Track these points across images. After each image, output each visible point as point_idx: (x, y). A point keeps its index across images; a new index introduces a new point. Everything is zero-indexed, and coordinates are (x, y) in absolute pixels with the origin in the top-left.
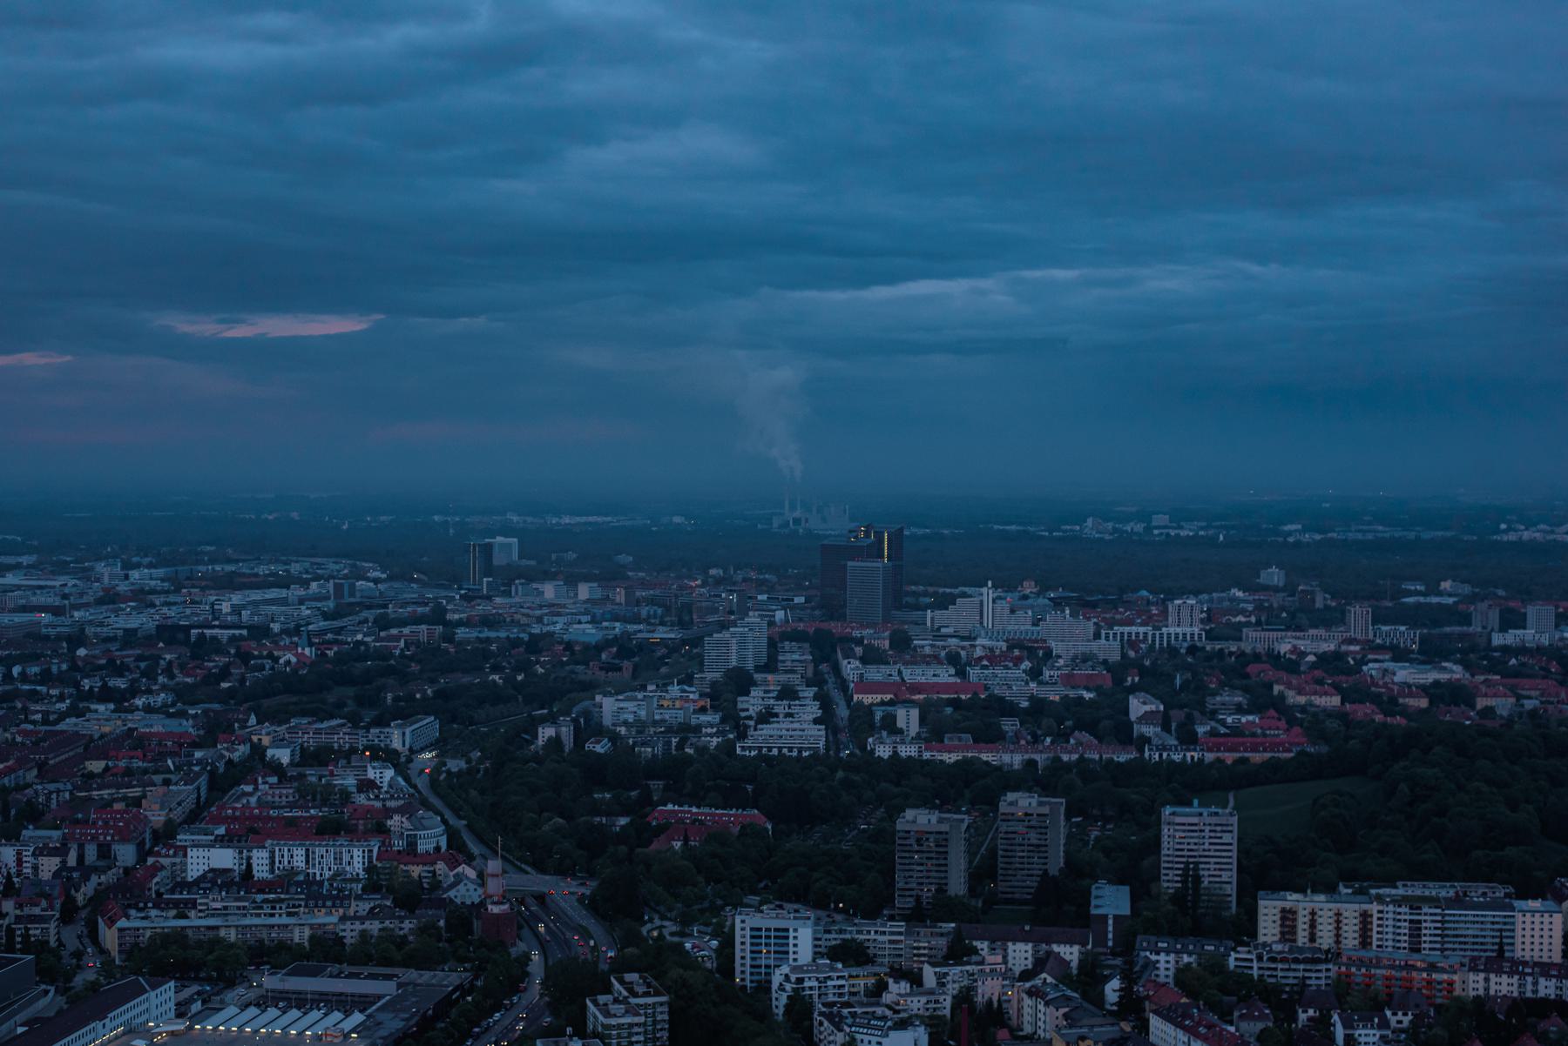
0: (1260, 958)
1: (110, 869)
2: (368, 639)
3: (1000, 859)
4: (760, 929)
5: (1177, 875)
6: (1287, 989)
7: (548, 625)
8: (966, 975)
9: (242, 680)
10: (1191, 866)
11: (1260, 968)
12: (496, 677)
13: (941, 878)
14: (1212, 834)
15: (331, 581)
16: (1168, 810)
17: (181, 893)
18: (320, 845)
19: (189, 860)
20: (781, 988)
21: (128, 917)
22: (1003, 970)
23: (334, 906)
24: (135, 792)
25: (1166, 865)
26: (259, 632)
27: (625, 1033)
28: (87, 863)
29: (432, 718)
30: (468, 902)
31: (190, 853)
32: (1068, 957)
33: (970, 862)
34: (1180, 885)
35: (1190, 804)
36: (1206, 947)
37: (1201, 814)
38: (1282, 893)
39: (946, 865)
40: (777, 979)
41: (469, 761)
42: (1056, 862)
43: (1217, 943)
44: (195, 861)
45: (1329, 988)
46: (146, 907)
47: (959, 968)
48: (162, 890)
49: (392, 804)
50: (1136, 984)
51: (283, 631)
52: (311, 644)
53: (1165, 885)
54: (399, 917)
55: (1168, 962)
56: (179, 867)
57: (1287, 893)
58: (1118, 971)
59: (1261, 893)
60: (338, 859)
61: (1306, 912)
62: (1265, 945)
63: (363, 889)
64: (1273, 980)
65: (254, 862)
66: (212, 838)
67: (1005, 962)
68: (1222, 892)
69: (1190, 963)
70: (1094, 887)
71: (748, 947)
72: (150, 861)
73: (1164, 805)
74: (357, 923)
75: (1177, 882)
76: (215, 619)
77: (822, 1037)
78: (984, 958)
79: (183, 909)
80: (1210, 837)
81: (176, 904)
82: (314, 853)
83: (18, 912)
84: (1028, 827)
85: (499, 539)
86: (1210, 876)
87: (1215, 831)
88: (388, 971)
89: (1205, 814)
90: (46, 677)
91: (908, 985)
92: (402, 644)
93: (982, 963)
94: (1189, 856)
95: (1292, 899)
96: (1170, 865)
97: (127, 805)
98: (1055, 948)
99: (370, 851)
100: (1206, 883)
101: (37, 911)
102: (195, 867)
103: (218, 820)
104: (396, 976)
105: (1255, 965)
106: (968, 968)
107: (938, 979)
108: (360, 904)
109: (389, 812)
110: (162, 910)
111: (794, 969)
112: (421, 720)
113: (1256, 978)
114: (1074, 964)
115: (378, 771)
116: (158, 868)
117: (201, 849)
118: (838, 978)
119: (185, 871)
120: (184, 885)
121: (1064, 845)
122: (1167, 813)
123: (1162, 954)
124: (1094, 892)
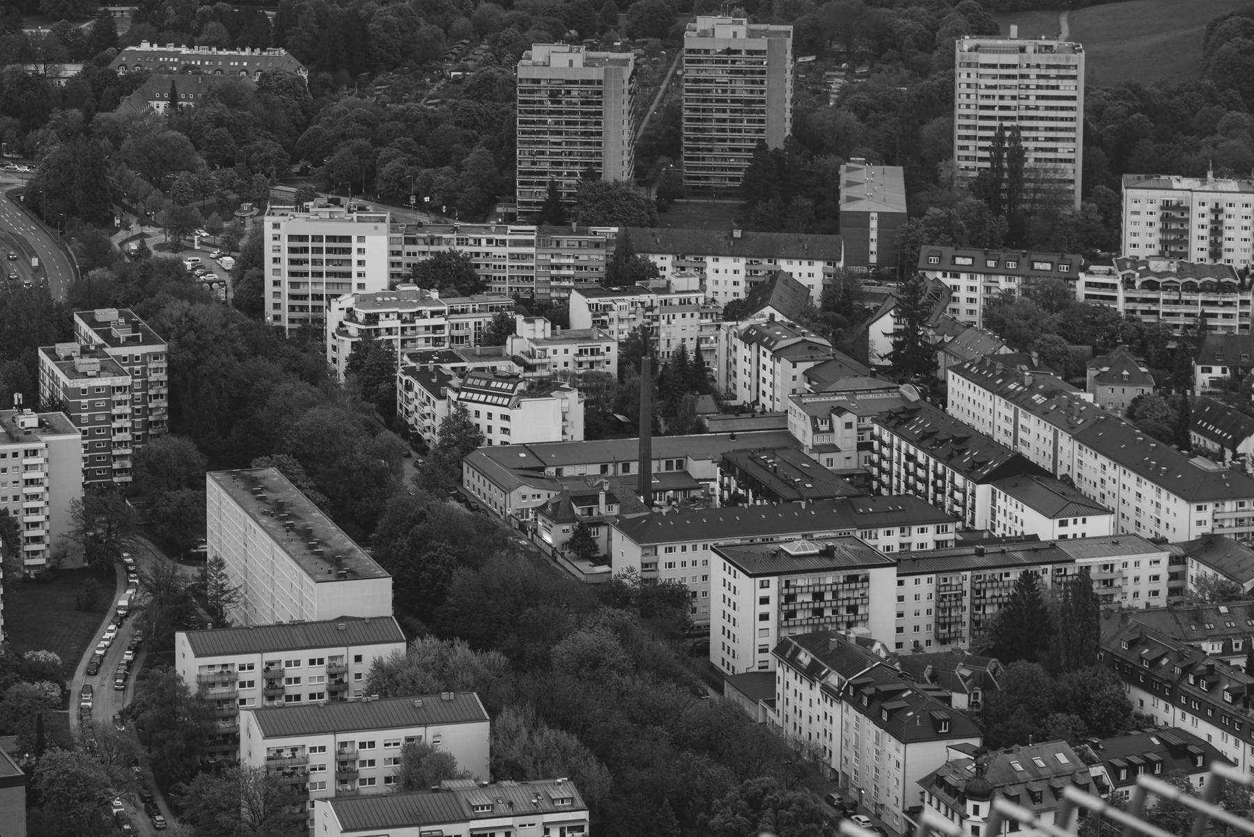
0: (1129, 283)
3: (685, 124)
4: (303, 238)
5: (981, 149)
6: (1177, 333)
8: (641, 310)
10: (1008, 134)
11: (1128, 300)
13: (592, 155)
14: (1043, 82)
16: (967, 43)
20: (342, 330)
22: (701, 301)
25: (964, 132)
27: (101, 402)
32: (805, 281)
33: (636, 130)
34: (988, 165)
35: (1006, 35)
36: (1037, 265)
37: (1022, 50)
38: (1163, 177)
39: (599, 134)
40: (333, 317)
42: (779, 130)
43: (1056, 259)
45: (1246, 333)
47: (629, 298)
50: (922, 324)
53: (963, 164)
55: (972, 289)
57: (1173, 178)
58: (892, 302)
59: (1126, 178)
61: (1205, 209)
62: (1135, 262)
64: (1151, 319)
67: (703, 288)
68: (1057, 177)
69: (1011, 291)
70: (843, 167)
71: (285, 267)
73: (959, 34)
75: (981, 159)
77: (411, 408)
78: (669, 282)
80: (1038, 87)
84: (731, 72)
86: (1036, 149)
87: (1047, 77)
89: (1030, 49)
91: (549, 325)
93: (666, 290)
94: (1002, 118)
95: (1181, 188)
96: (971, 132)
98: (784, 265)
100: (1031, 161)
105: (1121, 294)
106: (644, 298)
107: (594, 316)
111: (363, 300)
113: (1123, 314)
114: (816, 293)
118: (433, 314)
121: (792, 100)
122: (966, 47)
123: (964, 276)
124: (844, 177)
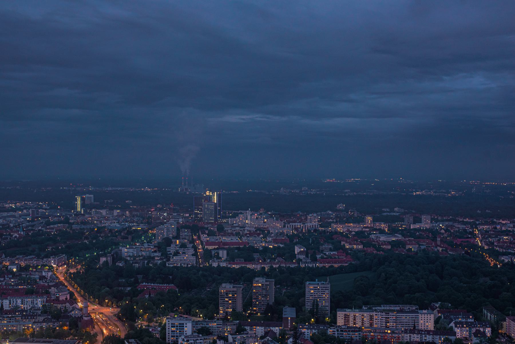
0: (338, 331)
2: (43, 229)
5: (311, 304)
6: (347, 340)
7: (103, 224)
8: (243, 338)
10: (315, 301)
11: (338, 334)
12: (86, 241)
13: (234, 306)
14: (322, 290)
15: (30, 209)
16: (308, 283)
18: (26, 298)
22: (254, 336)
25: (307, 301)
29: (64, 255)
30: (77, 316)
32: (275, 331)
33: (244, 301)
34: (312, 307)
35: (315, 281)
36: (320, 327)
37: (318, 284)
38: (345, 309)
39: (236, 302)
43: (324, 326)
45: (360, 340)
47: (240, 335)
49: (50, 284)
50: (298, 340)
51: (14, 226)
52: (23, 231)
53: (307, 307)
55: (308, 332)
57: (346, 309)
58: (292, 335)
59: (338, 309)
60: (32, 302)
62: (339, 326)
63: (41, 312)
64: (342, 338)
65: (4, 304)
68: (325, 309)
69: (315, 333)
70: (284, 308)
73: (306, 281)
75: (311, 306)
78: (248, 332)
80: (321, 291)
82: (24, 300)
84: (262, 289)
85: (87, 195)
87: (323, 289)
88: (50, 340)
89: (320, 284)
91: (223, 341)
92: (54, 230)
93: (247, 334)
94: (314, 298)
95: (348, 312)
96: (309, 301)
98: (271, 328)
100: (320, 306)
104: (52, 342)
105: (336, 333)
106: (243, 335)
107: (233, 339)
108: (40, 317)
109: (50, 287)
111: (186, 337)
112: (61, 256)
113: (336, 337)
114: (278, 334)
115: (46, 273)
118: (200, 339)
121: (274, 295)
122: (307, 284)
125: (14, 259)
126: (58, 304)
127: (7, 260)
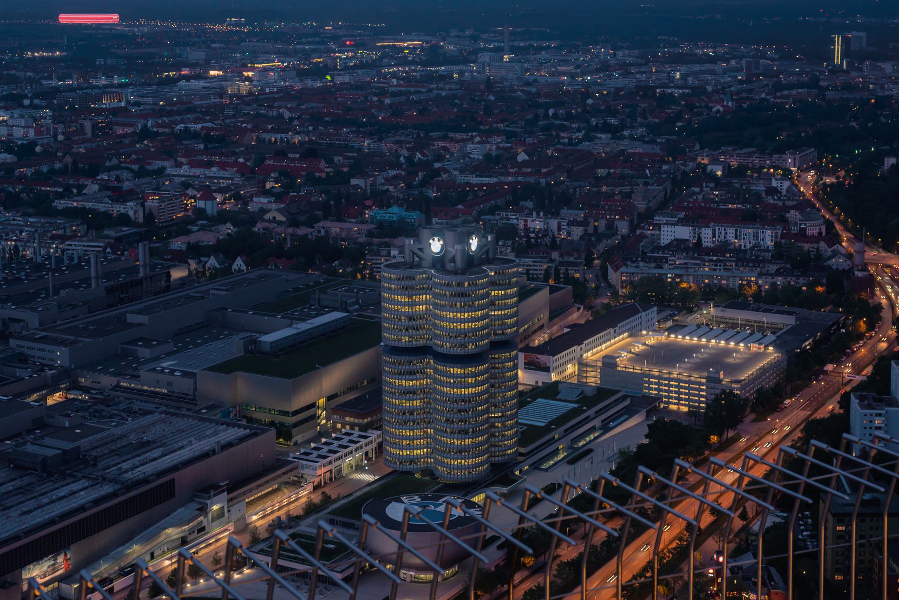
1: (614, 236)
2: (768, 97)
7: (888, 90)
9: (689, 121)
12: (854, 124)
15: (744, 59)
17: (658, 253)
18: (744, 227)
19: (662, 233)
21: (627, 266)
23: (754, 266)
24: (627, 189)
26: (698, 91)
28: (599, 232)
29: (813, 150)
30: (841, 269)
31: (663, 229)
41: (838, 178)
44: (666, 233)
46: (637, 260)
48: (645, 251)
49: (789, 203)
51: (713, 91)
52: (732, 100)
54: (797, 276)
56: (655, 237)
60: (756, 236)
63: (771, 256)
65: (703, 236)
66: (676, 219)
72: (638, 232)
74: (770, 277)
76: (672, 82)
79: (660, 263)
81: (655, 259)
82: (740, 232)
83: (560, 259)
85: (854, 33)
88: (791, 309)
90: (569, 117)
92: (791, 101)
97: (623, 197)
99: (776, 233)
101: (572, 259)
102: (665, 237)
103: (679, 209)
104: (795, 313)
108: (770, 266)
109: (787, 209)
110: (647, 262)
112: (806, 150)
115: (779, 182)
116: (643, 237)
117: (669, 226)
119: (660, 239)
120: (659, 248)
125: (717, 152)
126: (804, 242)
127: (705, 154)
